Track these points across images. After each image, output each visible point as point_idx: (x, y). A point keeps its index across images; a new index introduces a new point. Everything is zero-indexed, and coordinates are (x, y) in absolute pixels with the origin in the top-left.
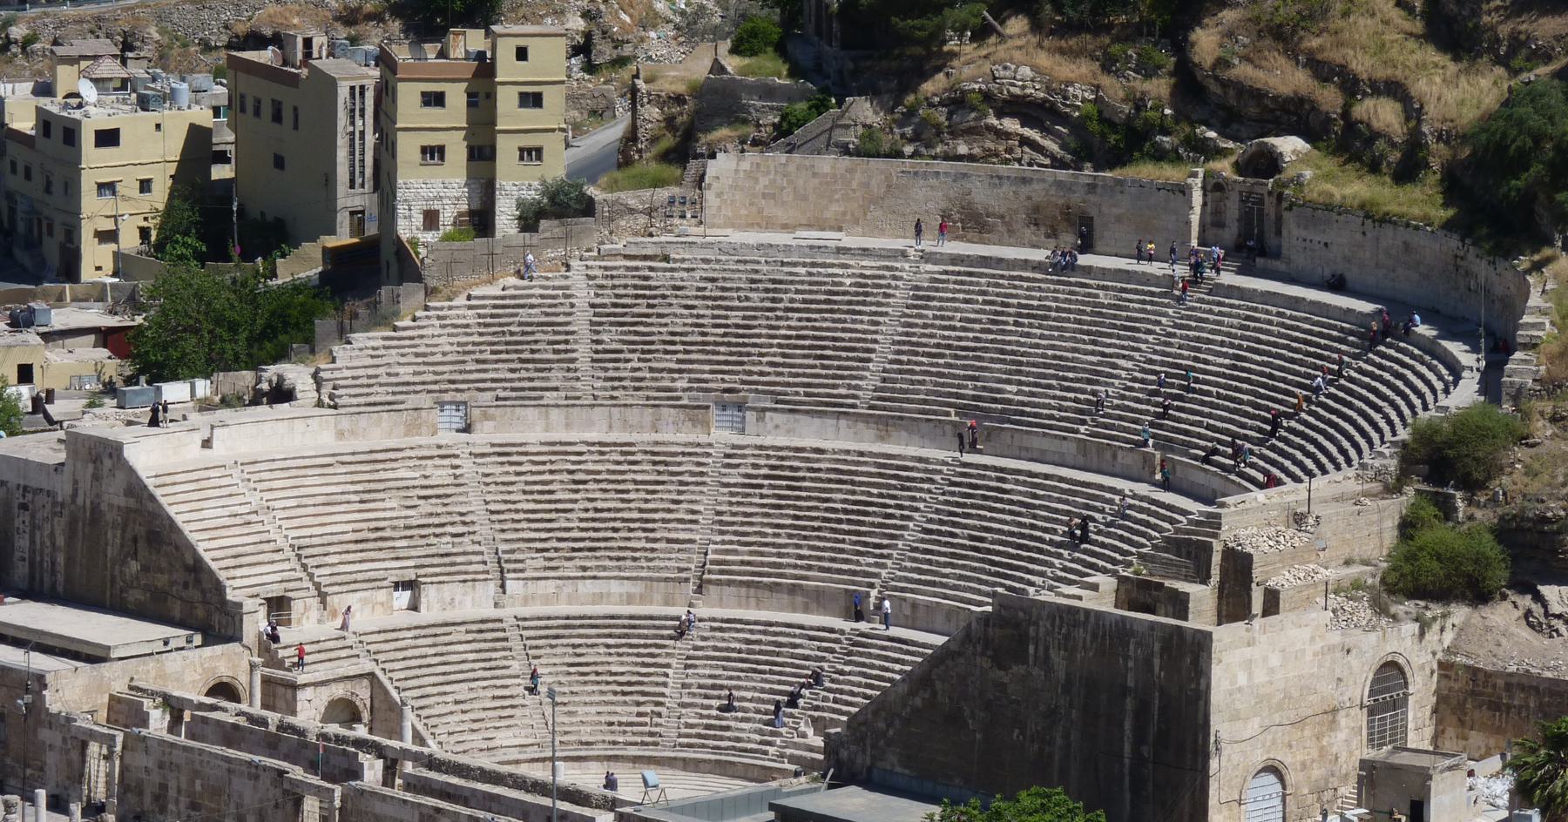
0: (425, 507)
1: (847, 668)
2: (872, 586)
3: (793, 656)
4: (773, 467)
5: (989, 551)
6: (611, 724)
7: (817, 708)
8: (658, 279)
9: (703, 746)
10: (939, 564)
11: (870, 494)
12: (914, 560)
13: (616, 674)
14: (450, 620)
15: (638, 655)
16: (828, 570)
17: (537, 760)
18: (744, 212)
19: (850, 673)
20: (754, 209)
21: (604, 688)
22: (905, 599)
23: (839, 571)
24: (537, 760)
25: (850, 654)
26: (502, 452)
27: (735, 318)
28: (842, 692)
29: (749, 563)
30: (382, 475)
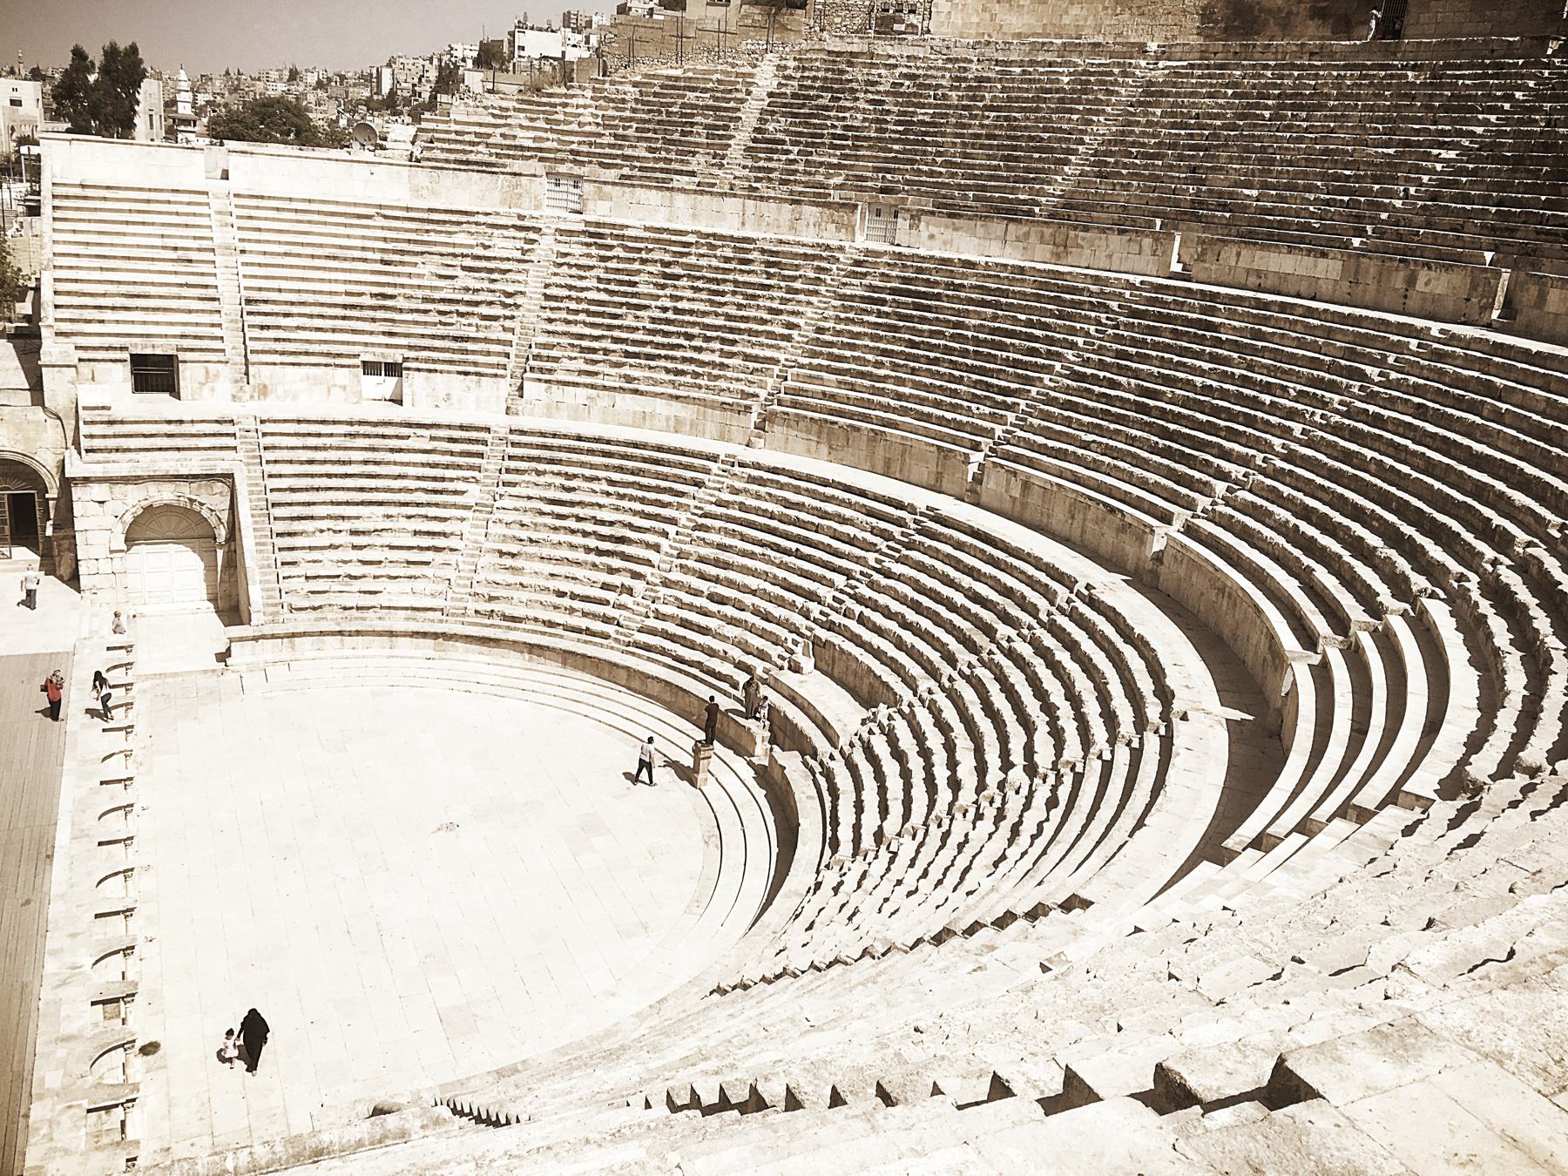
0: (467, 280)
1: (898, 568)
2: (976, 447)
3: (835, 536)
4: (906, 280)
5: (1163, 414)
6: (561, 594)
7: (831, 627)
8: (858, 73)
9: (663, 652)
10: (1081, 426)
11: (1016, 321)
12: (1047, 416)
13: (602, 523)
14: (607, 437)
15: (642, 500)
16: (927, 418)
17: (425, 635)
18: (975, 19)
19: (899, 578)
20: (988, 16)
21: (577, 540)
22: (1015, 473)
23: (941, 421)
24: (425, 635)
25: (910, 546)
26: (595, 234)
27: (923, 114)
28: (875, 607)
29: (833, 397)
30: (433, 237)
